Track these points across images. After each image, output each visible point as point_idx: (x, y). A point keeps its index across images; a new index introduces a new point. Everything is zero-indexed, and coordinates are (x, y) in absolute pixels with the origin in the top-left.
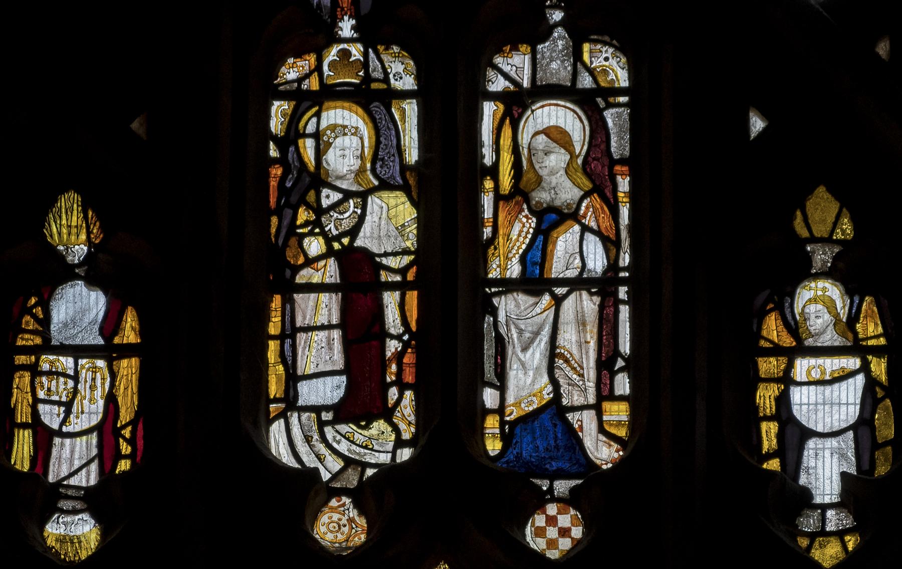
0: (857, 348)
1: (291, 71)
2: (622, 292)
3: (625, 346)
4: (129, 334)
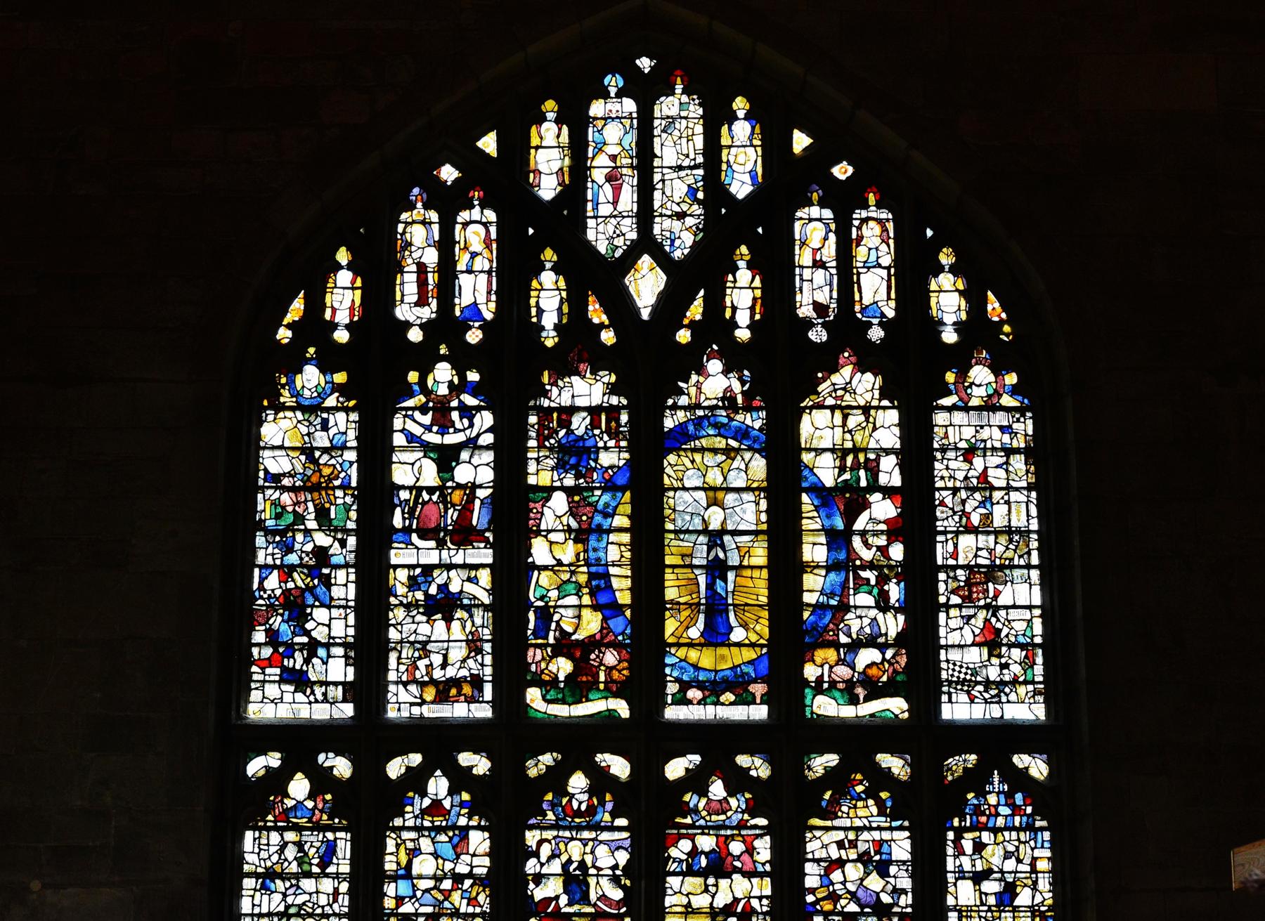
0: (558, 289)
1: (404, 216)
2: (494, 274)
3: (494, 287)
4: (359, 283)
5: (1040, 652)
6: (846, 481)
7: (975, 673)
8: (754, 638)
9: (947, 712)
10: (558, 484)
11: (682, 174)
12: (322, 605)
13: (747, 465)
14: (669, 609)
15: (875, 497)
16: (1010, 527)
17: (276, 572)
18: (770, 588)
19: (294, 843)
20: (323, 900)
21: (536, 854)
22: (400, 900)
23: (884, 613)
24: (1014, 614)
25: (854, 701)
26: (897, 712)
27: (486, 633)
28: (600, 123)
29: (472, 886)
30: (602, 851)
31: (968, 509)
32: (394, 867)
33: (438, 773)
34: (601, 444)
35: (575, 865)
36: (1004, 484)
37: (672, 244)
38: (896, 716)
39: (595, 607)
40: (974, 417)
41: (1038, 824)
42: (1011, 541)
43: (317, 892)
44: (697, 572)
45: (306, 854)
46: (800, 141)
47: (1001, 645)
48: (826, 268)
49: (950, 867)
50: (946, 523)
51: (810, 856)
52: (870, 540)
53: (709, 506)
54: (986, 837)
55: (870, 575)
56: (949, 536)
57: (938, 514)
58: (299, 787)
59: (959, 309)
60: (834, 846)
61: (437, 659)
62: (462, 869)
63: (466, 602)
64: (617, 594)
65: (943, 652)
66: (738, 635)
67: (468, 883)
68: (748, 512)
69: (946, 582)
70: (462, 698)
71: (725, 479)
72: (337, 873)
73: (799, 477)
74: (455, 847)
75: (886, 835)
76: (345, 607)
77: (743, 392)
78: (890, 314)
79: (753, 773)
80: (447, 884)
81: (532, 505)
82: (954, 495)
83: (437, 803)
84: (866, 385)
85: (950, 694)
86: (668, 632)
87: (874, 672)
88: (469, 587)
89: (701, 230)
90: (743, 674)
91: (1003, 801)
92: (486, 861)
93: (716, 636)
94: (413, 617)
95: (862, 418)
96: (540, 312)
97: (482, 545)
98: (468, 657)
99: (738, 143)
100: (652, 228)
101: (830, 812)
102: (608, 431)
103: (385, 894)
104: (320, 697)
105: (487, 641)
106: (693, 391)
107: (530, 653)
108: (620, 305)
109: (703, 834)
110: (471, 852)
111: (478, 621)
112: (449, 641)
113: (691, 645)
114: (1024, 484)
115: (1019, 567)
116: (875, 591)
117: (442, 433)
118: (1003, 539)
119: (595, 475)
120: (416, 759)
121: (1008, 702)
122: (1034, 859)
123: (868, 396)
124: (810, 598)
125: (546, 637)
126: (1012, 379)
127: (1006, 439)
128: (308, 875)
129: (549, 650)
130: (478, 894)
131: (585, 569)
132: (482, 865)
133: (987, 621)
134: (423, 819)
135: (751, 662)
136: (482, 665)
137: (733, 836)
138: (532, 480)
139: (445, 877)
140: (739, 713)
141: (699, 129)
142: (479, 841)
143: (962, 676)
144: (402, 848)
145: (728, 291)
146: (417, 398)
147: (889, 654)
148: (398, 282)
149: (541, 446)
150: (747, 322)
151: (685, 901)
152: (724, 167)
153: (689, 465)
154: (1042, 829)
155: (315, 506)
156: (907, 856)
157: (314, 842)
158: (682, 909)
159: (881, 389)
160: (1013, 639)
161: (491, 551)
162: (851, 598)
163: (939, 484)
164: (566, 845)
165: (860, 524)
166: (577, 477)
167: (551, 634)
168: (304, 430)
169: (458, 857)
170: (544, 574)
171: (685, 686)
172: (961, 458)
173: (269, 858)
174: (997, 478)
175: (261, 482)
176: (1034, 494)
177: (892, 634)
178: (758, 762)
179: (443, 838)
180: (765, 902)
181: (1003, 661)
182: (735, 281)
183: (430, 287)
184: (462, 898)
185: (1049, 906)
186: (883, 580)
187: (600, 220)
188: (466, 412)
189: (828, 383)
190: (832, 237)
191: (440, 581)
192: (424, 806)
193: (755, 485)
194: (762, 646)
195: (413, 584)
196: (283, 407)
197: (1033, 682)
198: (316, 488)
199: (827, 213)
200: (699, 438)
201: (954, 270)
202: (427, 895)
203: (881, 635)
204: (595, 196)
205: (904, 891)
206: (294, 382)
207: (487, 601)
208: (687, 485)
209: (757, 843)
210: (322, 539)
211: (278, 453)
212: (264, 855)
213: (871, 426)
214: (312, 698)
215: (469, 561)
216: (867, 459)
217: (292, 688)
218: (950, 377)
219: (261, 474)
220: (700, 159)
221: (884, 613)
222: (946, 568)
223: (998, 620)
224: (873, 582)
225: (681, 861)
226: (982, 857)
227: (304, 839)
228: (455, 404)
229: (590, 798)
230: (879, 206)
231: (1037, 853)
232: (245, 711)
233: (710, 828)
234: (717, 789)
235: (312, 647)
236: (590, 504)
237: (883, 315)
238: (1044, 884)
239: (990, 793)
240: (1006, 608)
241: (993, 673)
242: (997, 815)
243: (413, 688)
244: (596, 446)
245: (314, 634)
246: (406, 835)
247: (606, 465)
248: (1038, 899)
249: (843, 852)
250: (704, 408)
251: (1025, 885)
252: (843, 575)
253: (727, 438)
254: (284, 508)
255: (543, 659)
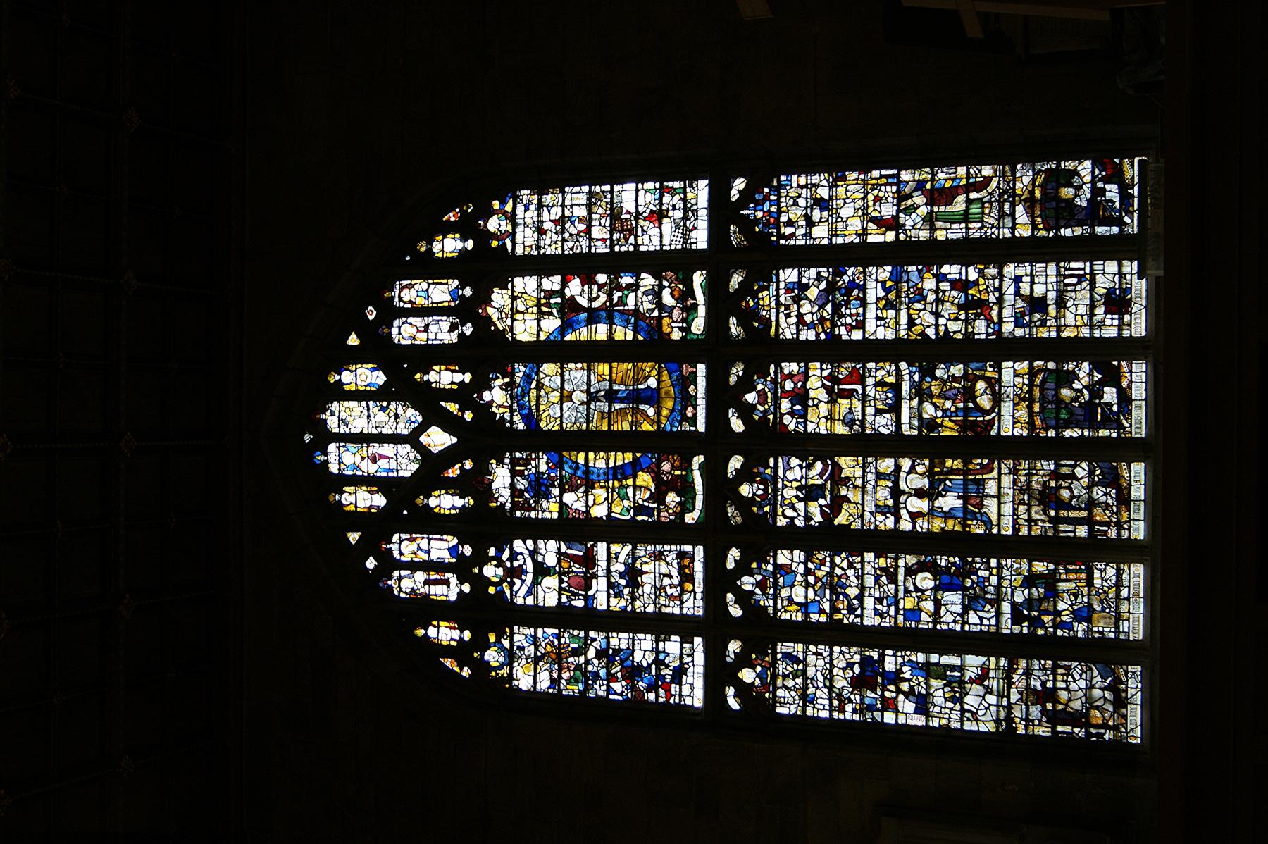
0: (440, 496)
2: (431, 536)
3: (438, 536)
4: (435, 623)
5: (665, 184)
6: (557, 311)
7: (678, 227)
8: (654, 372)
9: (703, 245)
10: (558, 498)
11: (372, 415)
12: (632, 655)
13: (547, 376)
14: (636, 428)
15: (568, 292)
16: (586, 205)
17: (611, 684)
18: (623, 362)
19: (783, 680)
20: (821, 663)
21: (792, 519)
22: (822, 611)
23: (640, 286)
24: (641, 202)
25: (695, 306)
26: (702, 278)
27: (650, 548)
28: (343, 467)
29: (812, 563)
30: (790, 475)
31: (575, 232)
32: (799, 614)
33: (739, 583)
34: (533, 470)
35: (799, 493)
36: (560, 209)
37: (414, 422)
38: (705, 278)
39: (635, 477)
40: (520, 229)
41: (775, 184)
42: (596, 204)
43: (816, 666)
44: (613, 409)
45: (791, 672)
46: (353, 340)
47: (661, 210)
48: (429, 324)
49: (803, 242)
50: (584, 247)
51: (795, 336)
52: (594, 296)
53: (572, 401)
54: (783, 219)
55: (616, 295)
56: (592, 244)
57: (578, 251)
58: (747, 675)
60: (788, 320)
61: (666, 581)
62: (801, 569)
63: (630, 561)
64: (626, 462)
65: (664, 248)
66: (652, 382)
67: (810, 565)
68: (576, 375)
69: (621, 246)
70: (691, 565)
71: (555, 390)
72: (803, 652)
73: (555, 342)
74: (787, 573)
75: (782, 285)
76: (634, 640)
77: (503, 378)
78: (456, 282)
79: (741, 373)
80: (811, 579)
81: (570, 516)
82: (566, 241)
83: (758, 584)
84: (500, 298)
85: (691, 243)
86: (651, 429)
87: (676, 293)
88: (622, 558)
89: (405, 404)
90: (677, 380)
91: (760, 207)
92: (796, 552)
93: (653, 397)
94: (640, 596)
95: (519, 300)
96: (453, 508)
97: (595, 549)
98: (665, 561)
99: (354, 379)
100: (404, 435)
101: (767, 322)
102: (526, 465)
103: (818, 621)
104: (690, 659)
105: (655, 547)
106: (502, 410)
107: (663, 519)
108: (450, 455)
109: (780, 408)
110: (790, 562)
111: (642, 553)
112: (655, 573)
113: (658, 413)
114: (560, 195)
115: (612, 198)
116: (626, 292)
117: (526, 572)
118: (594, 209)
119: (553, 474)
120: (730, 597)
121: (697, 204)
122: (799, 186)
123: (506, 297)
124: (630, 336)
125: (653, 509)
126: (496, 205)
127: (532, 207)
128: (804, 672)
129: (662, 507)
130: (817, 559)
131: (611, 482)
132: (798, 555)
133: (645, 219)
134: (768, 594)
135: (670, 374)
136: (670, 551)
137: (781, 388)
138: (555, 516)
139: (806, 580)
140: (702, 383)
141: (346, 404)
142: (783, 557)
143: (680, 235)
144: (788, 608)
145: (442, 387)
146: (505, 589)
147: (665, 283)
148: (435, 598)
149: (534, 509)
150: (460, 374)
151: (823, 420)
152: (368, 388)
153: (546, 413)
154: (779, 181)
155: (570, 657)
156: (796, 271)
157: (783, 667)
158: (829, 422)
159: (501, 289)
160: (657, 202)
161: (599, 543)
162: (630, 308)
163: (560, 251)
164: (786, 499)
165: (583, 302)
166: (554, 486)
167: (651, 505)
168: (524, 662)
169: (794, 571)
170: (613, 510)
171: (684, 418)
172: (544, 236)
173: (793, 697)
174: (556, 213)
175: (556, 691)
176: (567, 189)
177: (652, 281)
178: (734, 370)
179: (781, 580)
180: (824, 367)
181: (670, 208)
182: (436, 382)
183: (439, 577)
184: (820, 569)
185: (829, 175)
186: (619, 288)
187: (399, 468)
188: (514, 556)
189: (497, 323)
190: (411, 320)
191: (617, 578)
192: (760, 593)
193: (559, 370)
194: (660, 367)
195: (619, 595)
196: (510, 674)
197: (685, 188)
198: (559, 655)
199: (396, 323)
200: (530, 407)
201: (430, 242)
202: (818, 593)
203: (654, 288)
204: (385, 470)
205: (819, 273)
206: (494, 667)
207: (630, 547)
208: (558, 414)
209: (786, 372)
210: (591, 653)
211: (538, 680)
212: (791, 700)
213: (524, 295)
214: (691, 664)
215: (605, 558)
216: (545, 298)
217: (684, 677)
218: (495, 244)
219: (551, 691)
220: (364, 403)
221: (640, 286)
222: (612, 247)
223: (645, 212)
224: (620, 294)
225: (798, 422)
226: (797, 221)
227: (781, 673)
228: (508, 564)
229: (756, 482)
230: (392, 290)
231: (795, 184)
232: (698, 708)
233: (776, 403)
234: (751, 397)
235: (658, 663)
236: (570, 478)
237: (457, 288)
238: (815, 179)
239: (755, 216)
240: (637, 206)
241: (678, 214)
242: (769, 211)
243: (685, 597)
244: (535, 474)
245: (650, 661)
246: (779, 606)
247: (546, 467)
248: (825, 183)
249: (792, 314)
250: (512, 403)
251: (815, 191)
252: (616, 313)
253: (530, 389)
254: (571, 677)
255: (667, 511)
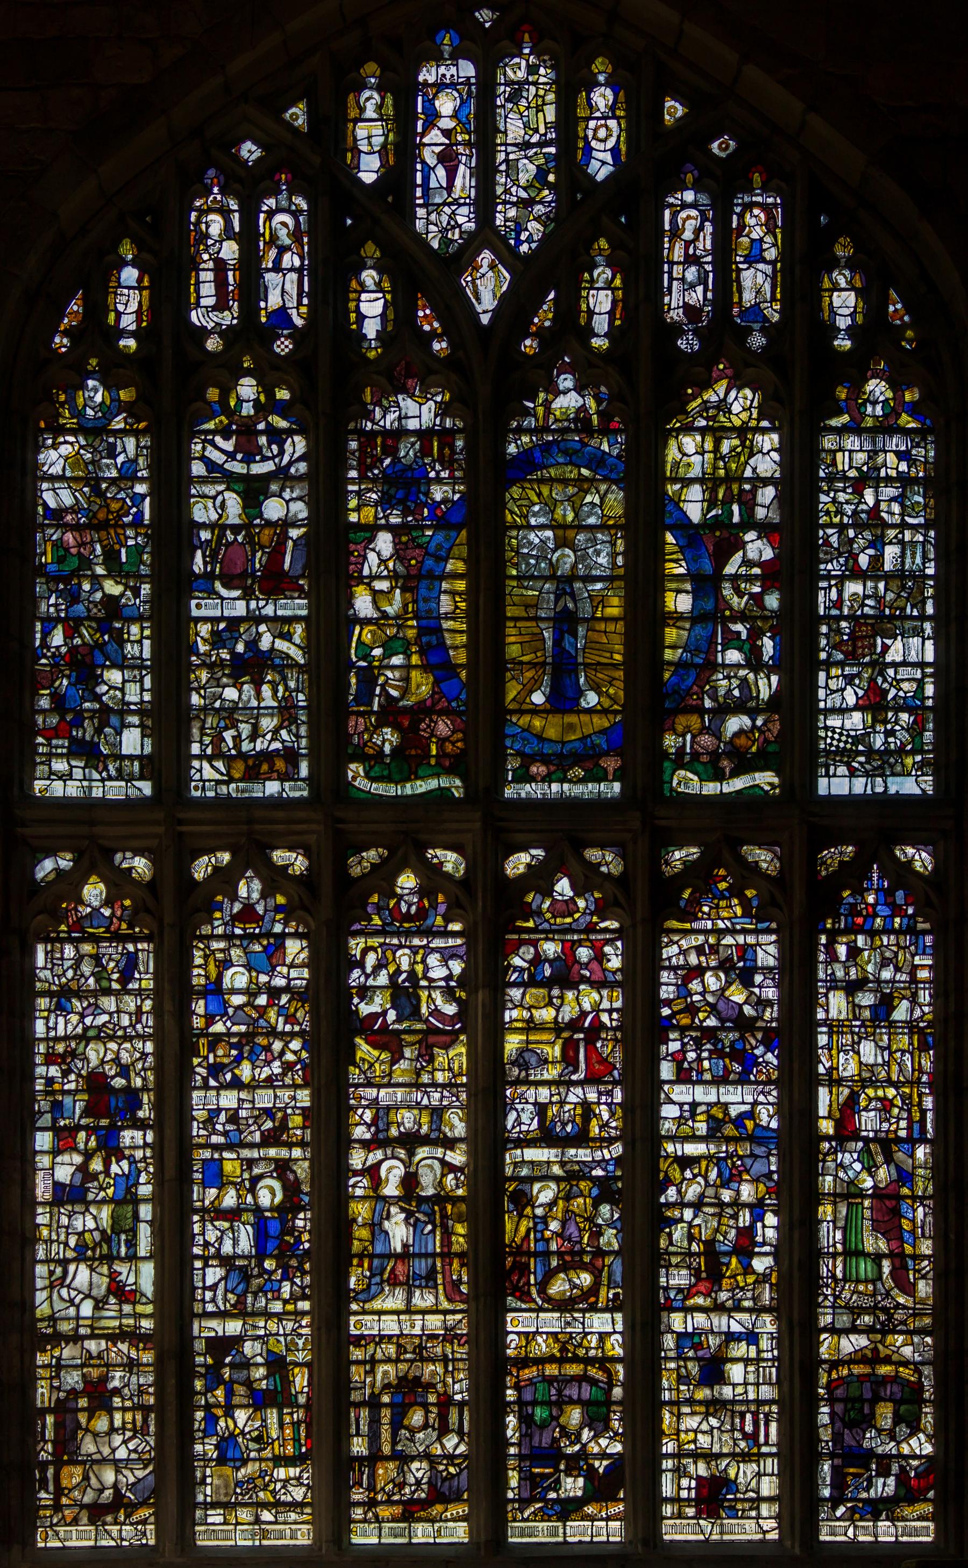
59: (855, 311)
145: (584, 293)
182: (592, 281)
